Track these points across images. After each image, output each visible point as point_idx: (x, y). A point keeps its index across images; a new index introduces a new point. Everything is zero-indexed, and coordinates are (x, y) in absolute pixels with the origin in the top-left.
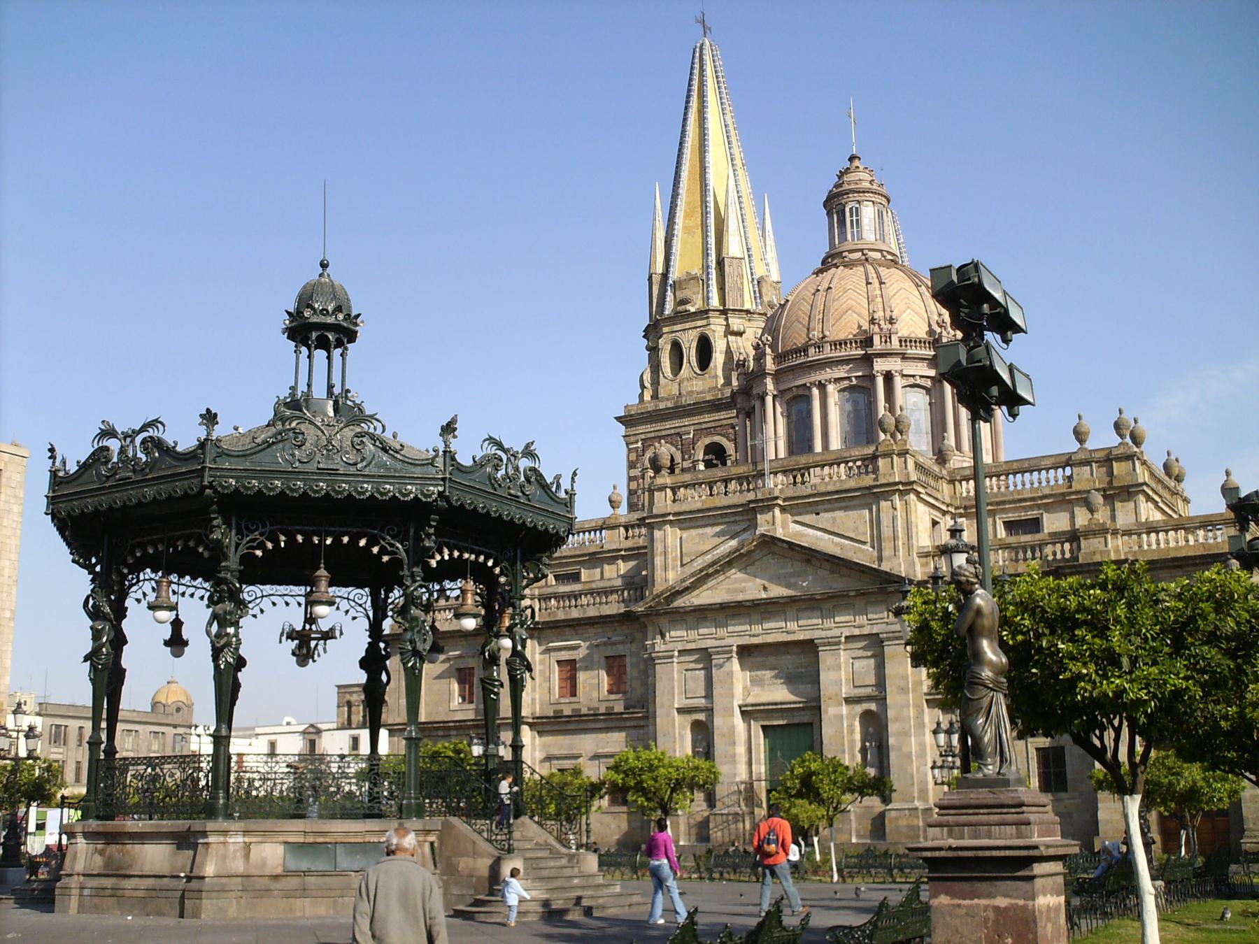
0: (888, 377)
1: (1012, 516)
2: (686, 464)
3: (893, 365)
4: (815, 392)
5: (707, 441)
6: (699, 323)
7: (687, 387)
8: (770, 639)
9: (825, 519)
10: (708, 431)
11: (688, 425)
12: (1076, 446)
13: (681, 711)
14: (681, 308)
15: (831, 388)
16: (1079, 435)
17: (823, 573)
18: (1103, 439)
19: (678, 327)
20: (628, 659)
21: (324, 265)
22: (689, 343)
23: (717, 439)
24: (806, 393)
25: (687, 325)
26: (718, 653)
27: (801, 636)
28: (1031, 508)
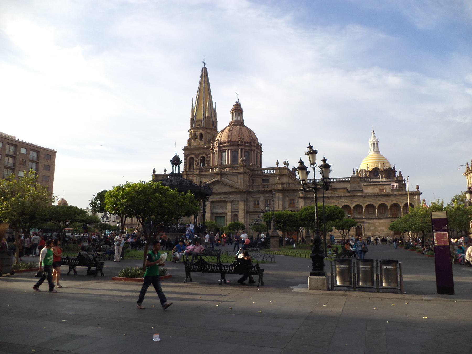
0: (241, 150)
1: (264, 178)
3: (243, 147)
8: (218, 200)
10: (202, 154)
17: (229, 188)
18: (281, 165)
22: (198, 133)
27: (224, 199)
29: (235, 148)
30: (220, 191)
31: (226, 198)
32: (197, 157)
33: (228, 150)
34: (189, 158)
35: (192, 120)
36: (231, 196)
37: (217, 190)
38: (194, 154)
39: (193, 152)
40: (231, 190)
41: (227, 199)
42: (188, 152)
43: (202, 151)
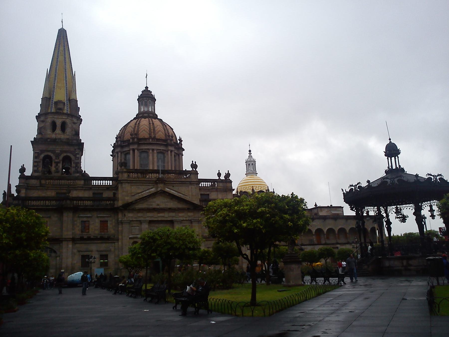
2: (57, 161)
4: (151, 151)
5: (65, 154)
6: (64, 117)
7: (59, 136)
8: (160, 219)
9: (176, 188)
10: (66, 152)
11: (58, 149)
12: (218, 178)
13: (130, 238)
14: (58, 111)
15: (155, 151)
16: (219, 175)
19: (55, 117)
20: (109, 222)
21: (390, 139)
23: (69, 154)
24: (148, 151)
25: (60, 117)
26: (144, 222)
28: (208, 191)
29: (162, 148)
30: (163, 206)
31: (173, 217)
32: (58, 156)
33: (153, 150)
34: (42, 156)
35: (46, 100)
36: (180, 215)
37: (158, 205)
38: (53, 152)
39: (51, 148)
40: (180, 206)
41: (174, 219)
42: (43, 147)
43: (66, 148)
